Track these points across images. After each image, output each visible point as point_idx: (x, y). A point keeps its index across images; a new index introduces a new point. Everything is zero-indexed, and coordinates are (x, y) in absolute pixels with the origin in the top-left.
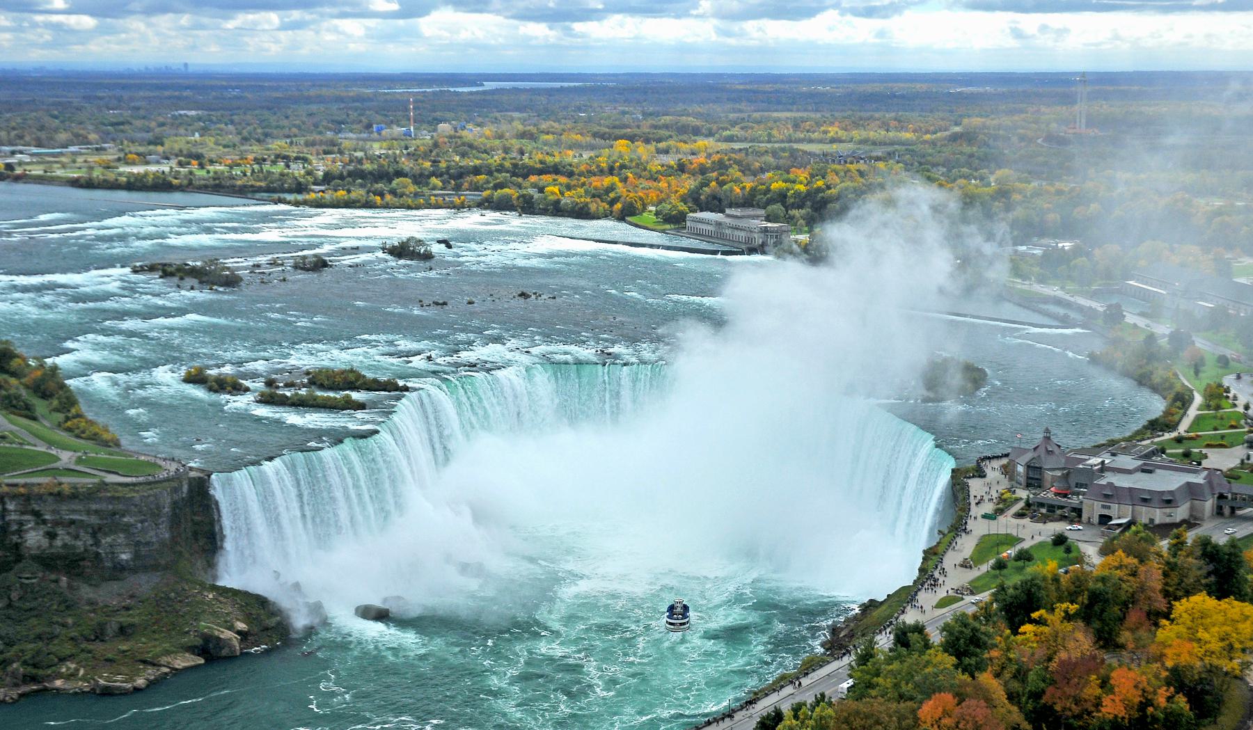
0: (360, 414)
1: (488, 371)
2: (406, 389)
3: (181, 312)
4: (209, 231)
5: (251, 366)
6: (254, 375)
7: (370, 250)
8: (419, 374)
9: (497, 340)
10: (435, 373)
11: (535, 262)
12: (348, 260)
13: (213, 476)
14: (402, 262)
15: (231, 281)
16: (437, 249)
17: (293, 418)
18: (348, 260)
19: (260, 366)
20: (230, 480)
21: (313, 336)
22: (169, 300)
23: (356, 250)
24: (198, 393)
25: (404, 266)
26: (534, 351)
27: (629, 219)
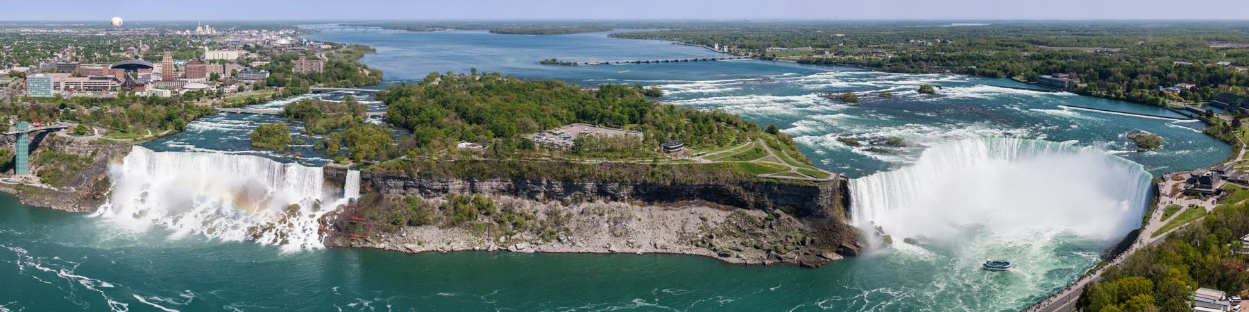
0: (907, 157)
1: (958, 140)
2: (925, 147)
3: (837, 113)
4: (847, 81)
5: (863, 136)
6: (865, 139)
7: (910, 89)
8: (931, 140)
9: (961, 127)
10: (937, 141)
11: (978, 96)
12: (901, 93)
13: (850, 180)
14: (922, 95)
15: (854, 100)
16: (936, 89)
17: (880, 157)
18: (901, 93)
19: (867, 136)
20: (856, 182)
21: (888, 124)
22: (832, 108)
23: (904, 90)
24: (841, 145)
25: (923, 96)
26: (977, 131)
27: (1013, 78)
